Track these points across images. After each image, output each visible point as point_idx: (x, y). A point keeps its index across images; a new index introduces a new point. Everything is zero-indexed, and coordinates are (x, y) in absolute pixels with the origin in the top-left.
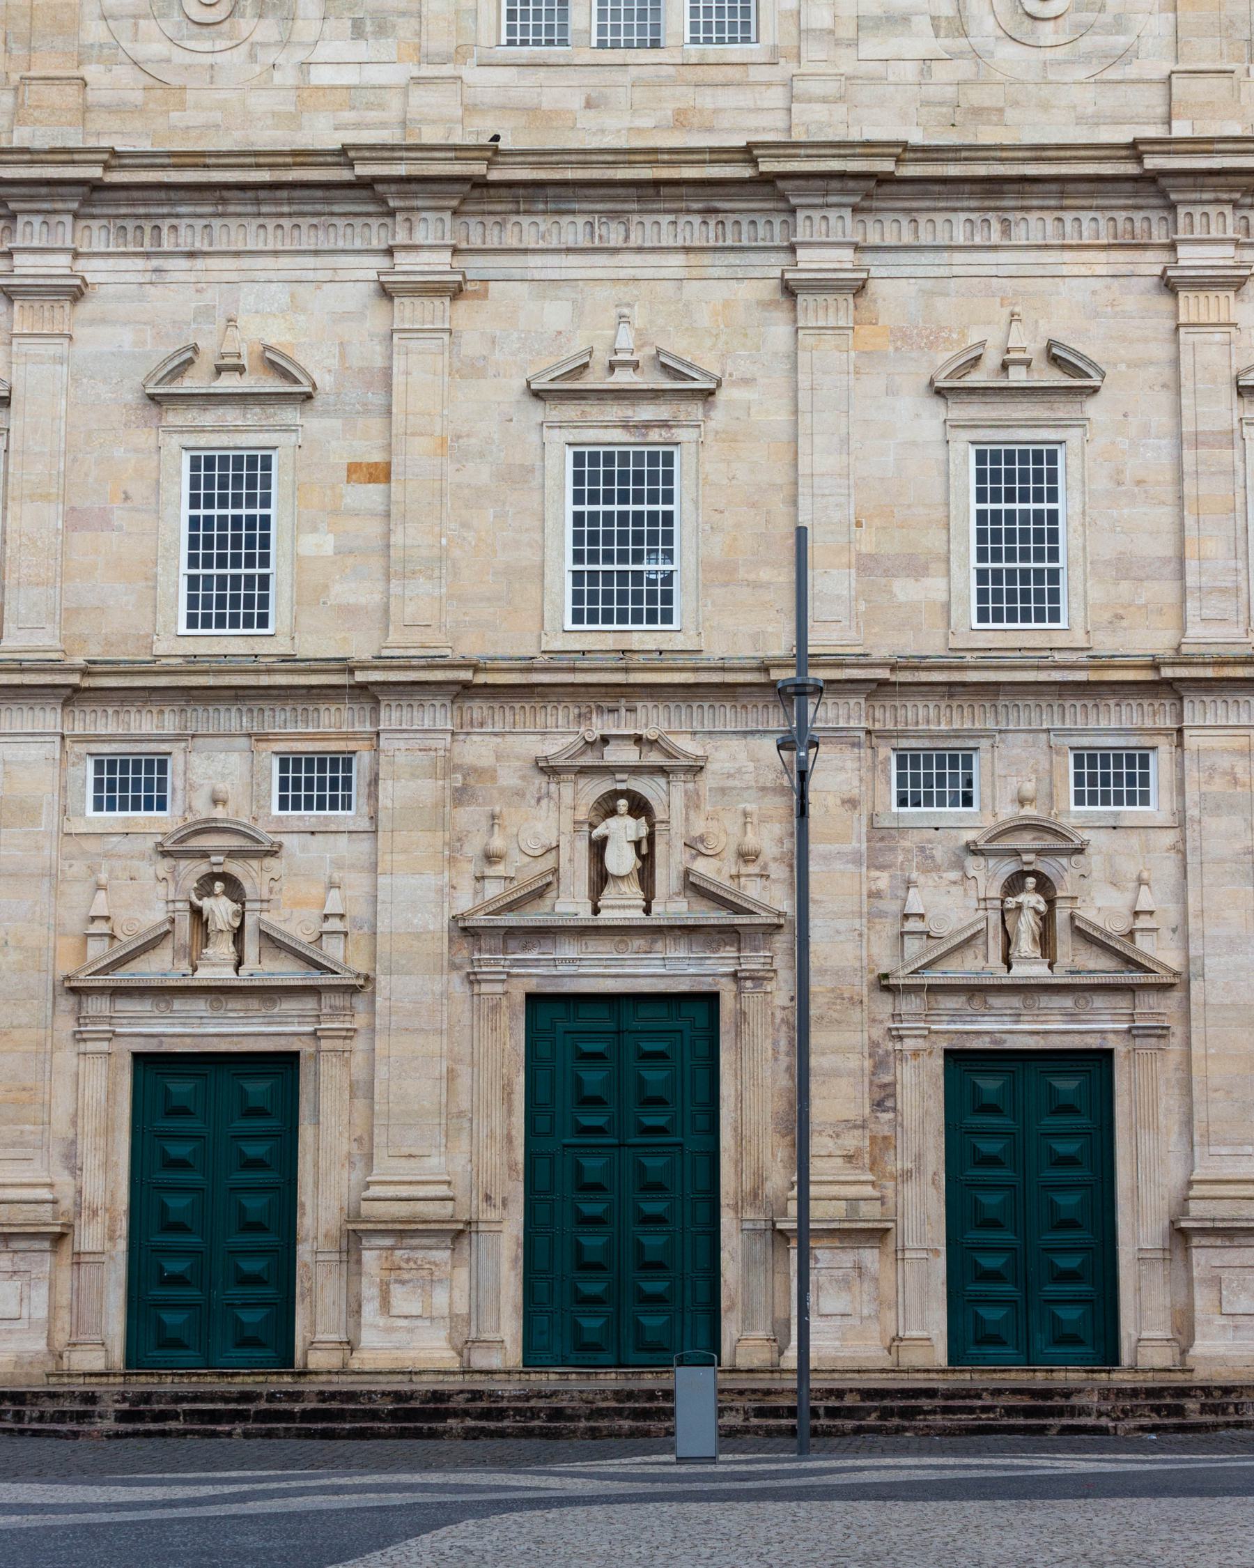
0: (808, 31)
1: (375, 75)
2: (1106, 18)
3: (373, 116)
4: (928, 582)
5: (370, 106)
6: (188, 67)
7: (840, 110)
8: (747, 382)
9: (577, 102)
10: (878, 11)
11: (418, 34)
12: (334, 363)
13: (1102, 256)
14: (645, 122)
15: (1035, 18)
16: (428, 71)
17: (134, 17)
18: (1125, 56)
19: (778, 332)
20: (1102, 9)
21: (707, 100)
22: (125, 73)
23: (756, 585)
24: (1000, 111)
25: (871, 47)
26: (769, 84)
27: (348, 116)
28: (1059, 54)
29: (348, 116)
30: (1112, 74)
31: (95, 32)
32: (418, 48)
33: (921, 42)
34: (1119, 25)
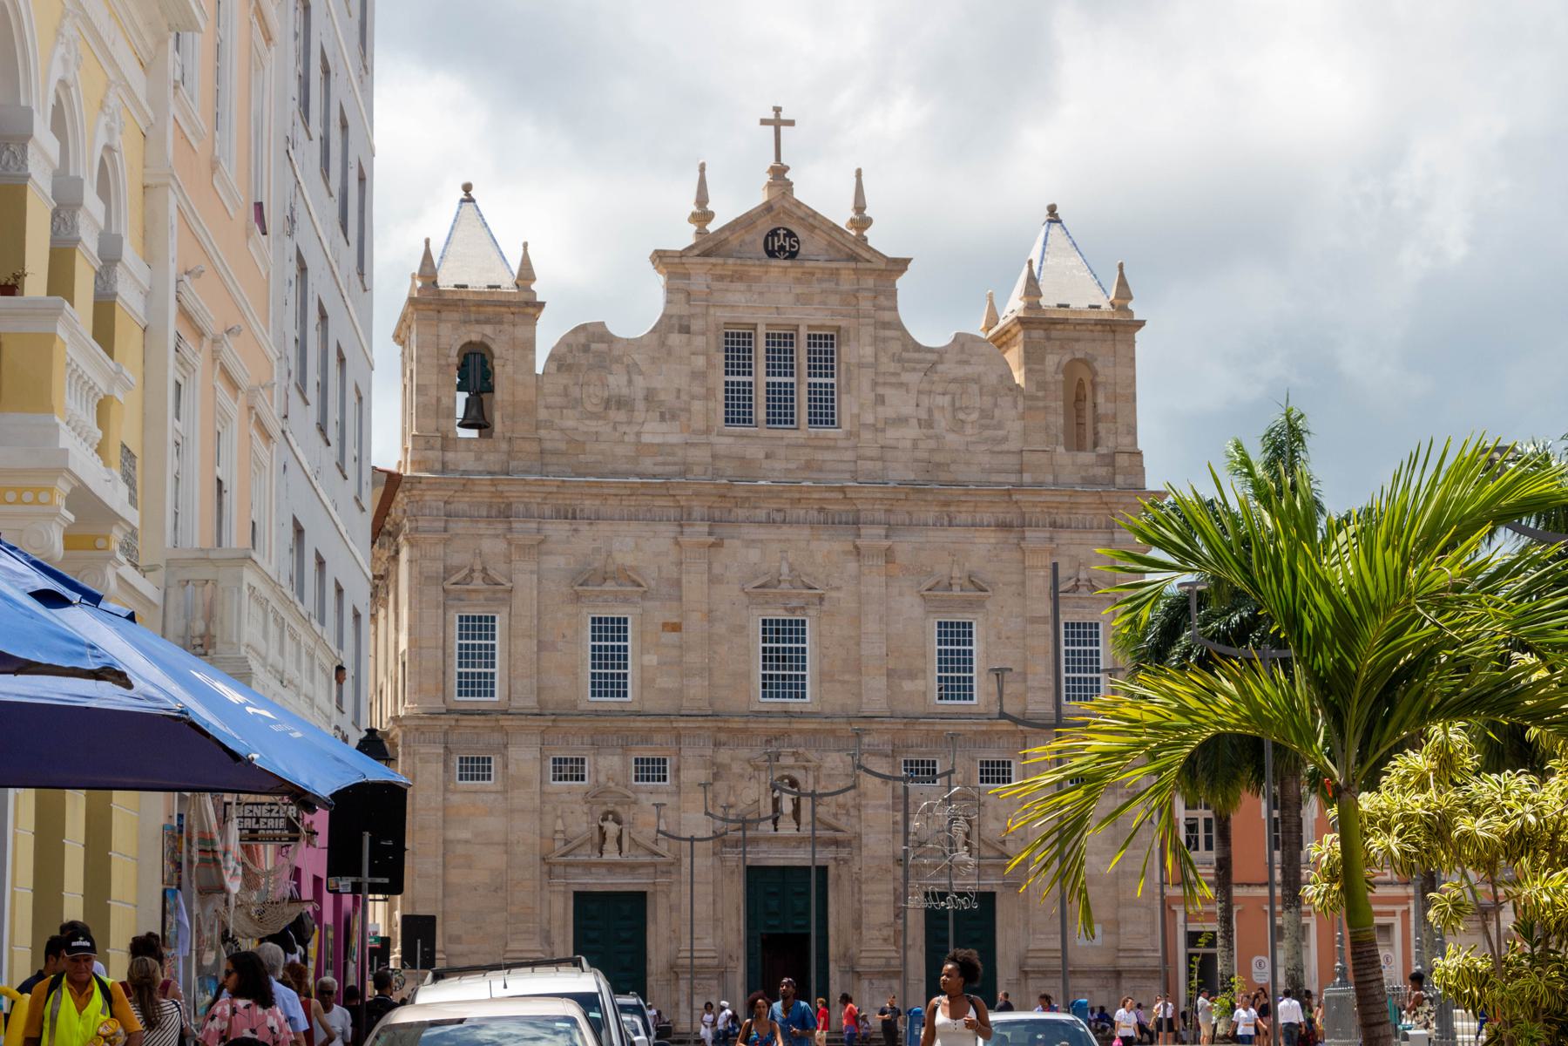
0: (864, 425)
1: (674, 439)
2: (995, 422)
3: (670, 459)
4: (917, 682)
5: (669, 454)
6: (586, 433)
7: (879, 464)
8: (838, 589)
9: (762, 455)
10: (894, 416)
11: (689, 420)
12: (656, 575)
13: (993, 535)
14: (792, 466)
15: (962, 421)
16: (695, 439)
17: (562, 408)
18: (1005, 439)
19: (852, 566)
20: (993, 418)
21: (820, 456)
22: (556, 434)
23: (843, 682)
24: (948, 465)
25: (892, 434)
26: (846, 449)
27: (660, 459)
28: (973, 439)
29: (660, 459)
30: (996, 449)
31: (543, 414)
32: (689, 426)
33: (912, 432)
34: (999, 426)
